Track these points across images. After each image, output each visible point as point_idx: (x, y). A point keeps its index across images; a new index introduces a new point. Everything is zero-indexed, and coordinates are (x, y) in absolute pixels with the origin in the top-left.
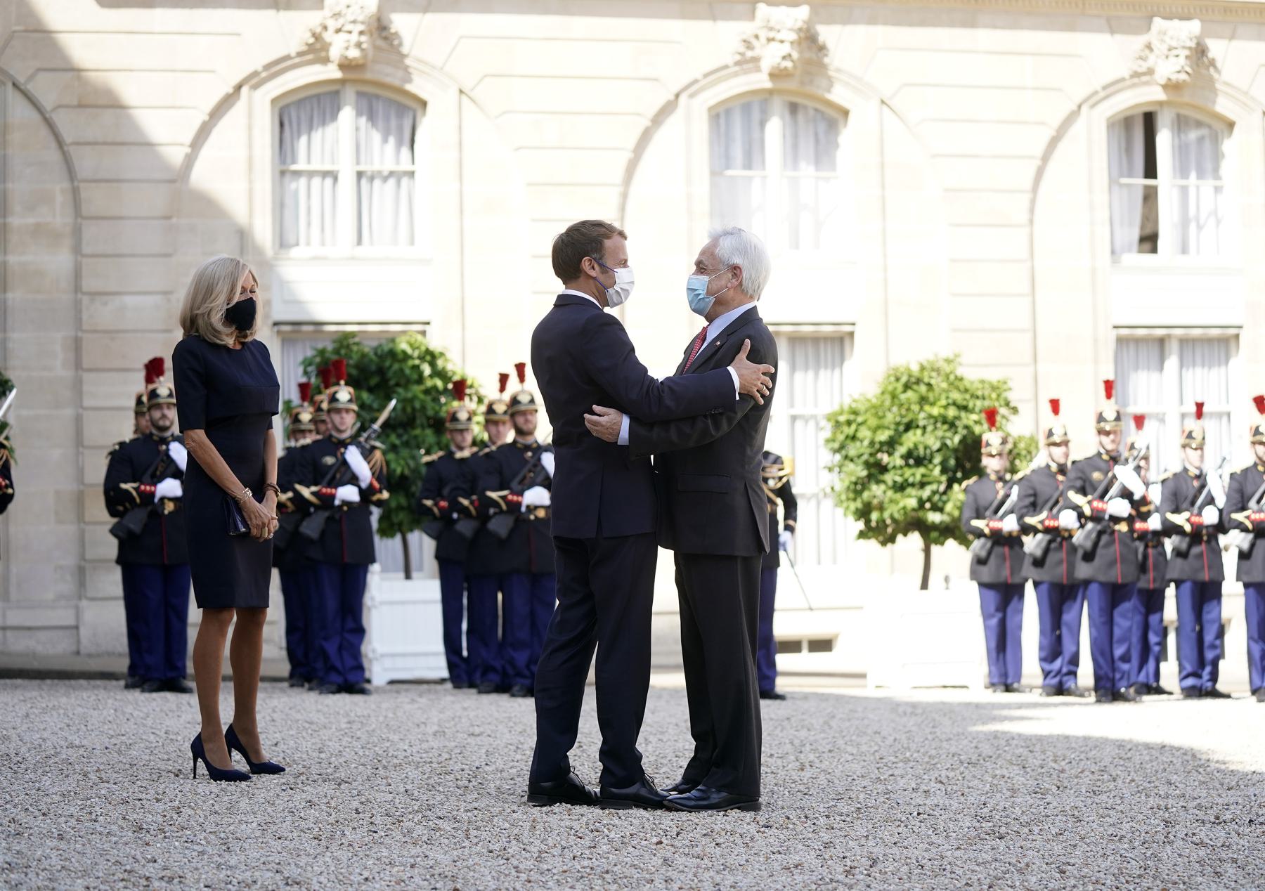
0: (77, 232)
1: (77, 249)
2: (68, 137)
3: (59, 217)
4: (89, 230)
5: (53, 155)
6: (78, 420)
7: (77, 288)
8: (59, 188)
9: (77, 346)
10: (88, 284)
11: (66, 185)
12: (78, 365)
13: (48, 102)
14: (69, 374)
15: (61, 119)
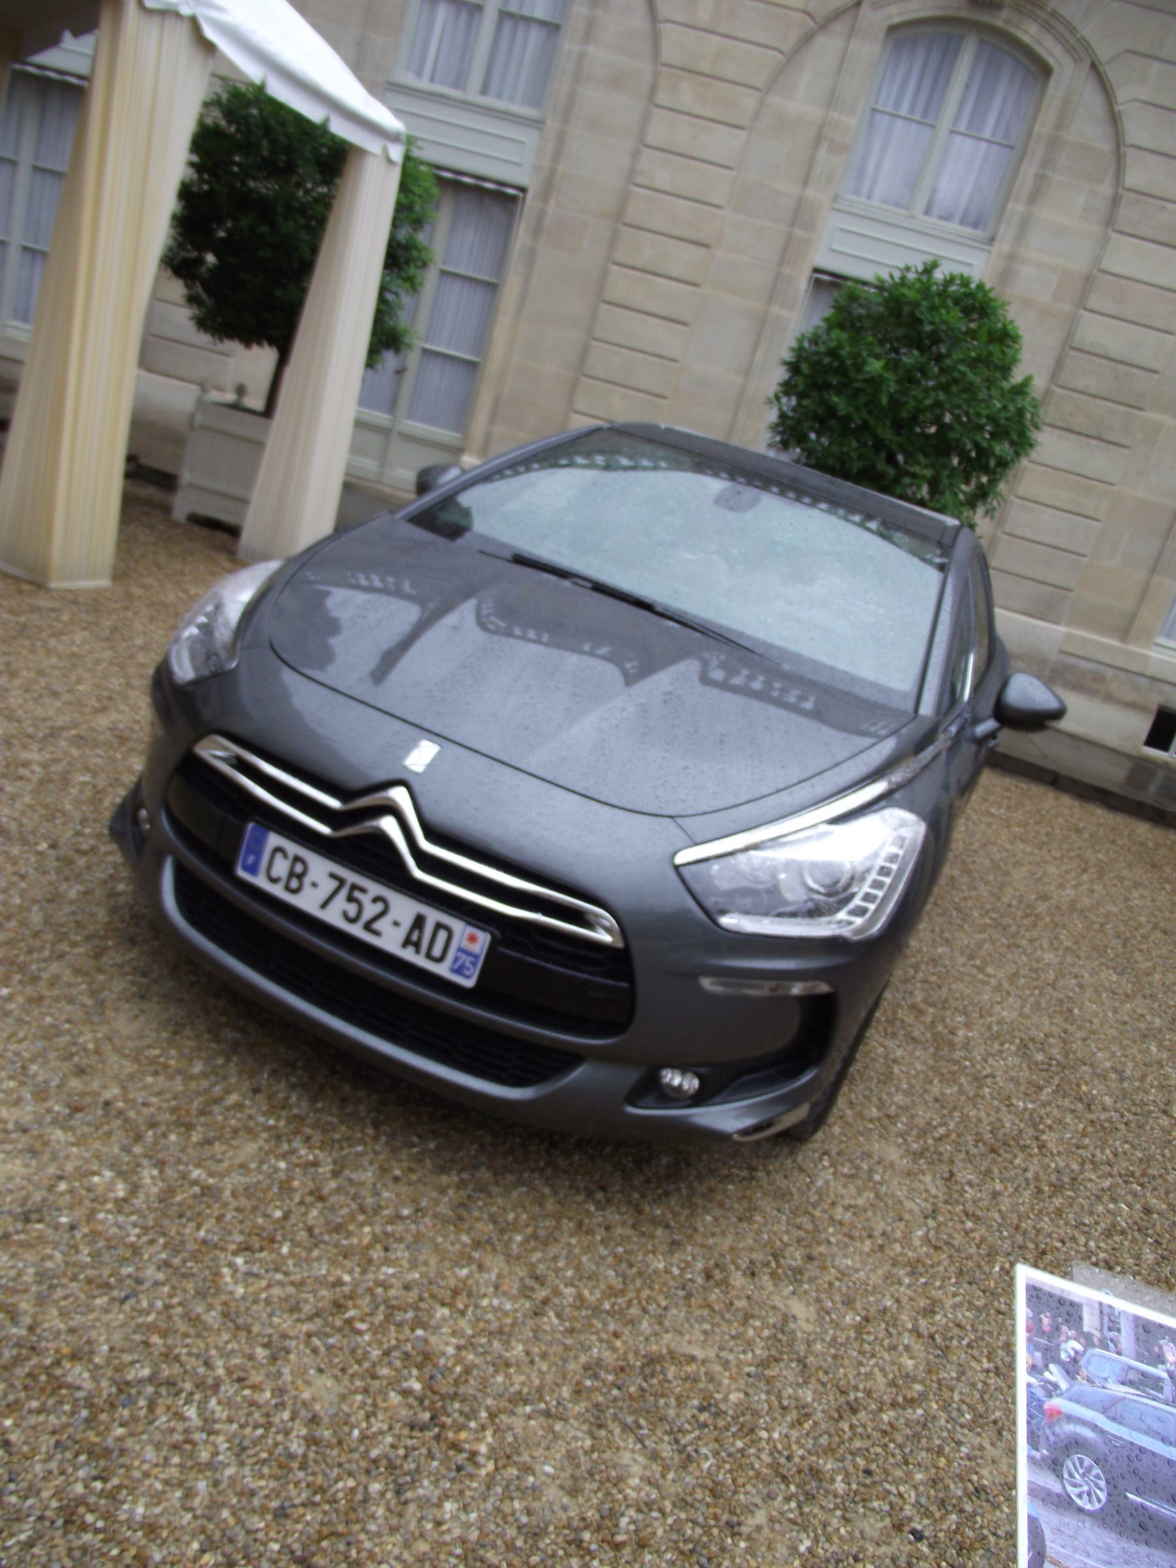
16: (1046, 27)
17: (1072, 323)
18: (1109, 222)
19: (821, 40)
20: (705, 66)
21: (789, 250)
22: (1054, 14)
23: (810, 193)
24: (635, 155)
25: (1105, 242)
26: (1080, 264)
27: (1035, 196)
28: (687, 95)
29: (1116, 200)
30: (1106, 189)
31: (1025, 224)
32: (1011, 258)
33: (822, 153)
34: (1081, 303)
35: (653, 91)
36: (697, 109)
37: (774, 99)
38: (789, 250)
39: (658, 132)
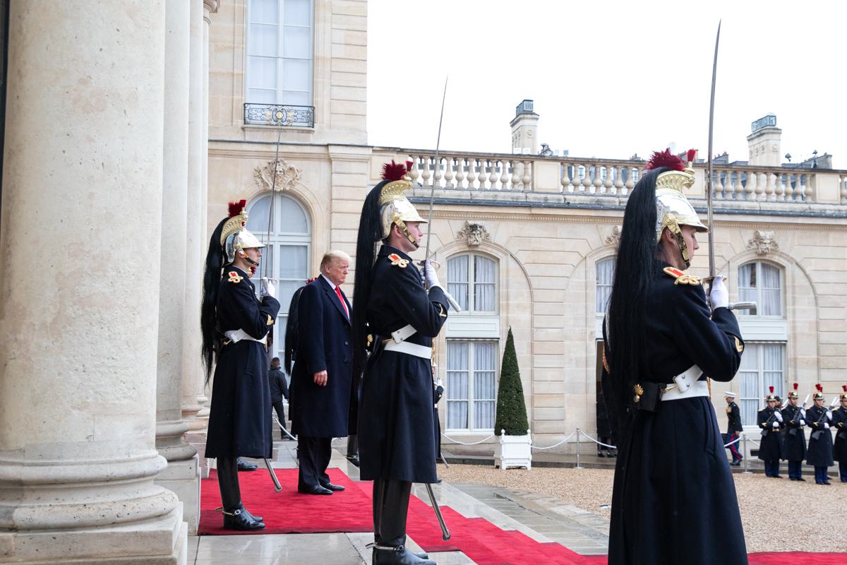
0: (532, 306)
1: (532, 312)
2: (529, 273)
3: (526, 301)
4: (537, 306)
5: (524, 280)
6: (532, 371)
7: (532, 326)
8: (526, 291)
9: (532, 346)
10: (536, 325)
11: (528, 290)
12: (532, 352)
13: (522, 262)
14: (529, 355)
15: (527, 268)
16: (780, 256)
18: (817, 304)
22: (781, 253)
26: (813, 318)
27: (794, 304)
29: (816, 298)
30: (812, 295)
31: (794, 311)
32: (794, 322)
34: (817, 330)
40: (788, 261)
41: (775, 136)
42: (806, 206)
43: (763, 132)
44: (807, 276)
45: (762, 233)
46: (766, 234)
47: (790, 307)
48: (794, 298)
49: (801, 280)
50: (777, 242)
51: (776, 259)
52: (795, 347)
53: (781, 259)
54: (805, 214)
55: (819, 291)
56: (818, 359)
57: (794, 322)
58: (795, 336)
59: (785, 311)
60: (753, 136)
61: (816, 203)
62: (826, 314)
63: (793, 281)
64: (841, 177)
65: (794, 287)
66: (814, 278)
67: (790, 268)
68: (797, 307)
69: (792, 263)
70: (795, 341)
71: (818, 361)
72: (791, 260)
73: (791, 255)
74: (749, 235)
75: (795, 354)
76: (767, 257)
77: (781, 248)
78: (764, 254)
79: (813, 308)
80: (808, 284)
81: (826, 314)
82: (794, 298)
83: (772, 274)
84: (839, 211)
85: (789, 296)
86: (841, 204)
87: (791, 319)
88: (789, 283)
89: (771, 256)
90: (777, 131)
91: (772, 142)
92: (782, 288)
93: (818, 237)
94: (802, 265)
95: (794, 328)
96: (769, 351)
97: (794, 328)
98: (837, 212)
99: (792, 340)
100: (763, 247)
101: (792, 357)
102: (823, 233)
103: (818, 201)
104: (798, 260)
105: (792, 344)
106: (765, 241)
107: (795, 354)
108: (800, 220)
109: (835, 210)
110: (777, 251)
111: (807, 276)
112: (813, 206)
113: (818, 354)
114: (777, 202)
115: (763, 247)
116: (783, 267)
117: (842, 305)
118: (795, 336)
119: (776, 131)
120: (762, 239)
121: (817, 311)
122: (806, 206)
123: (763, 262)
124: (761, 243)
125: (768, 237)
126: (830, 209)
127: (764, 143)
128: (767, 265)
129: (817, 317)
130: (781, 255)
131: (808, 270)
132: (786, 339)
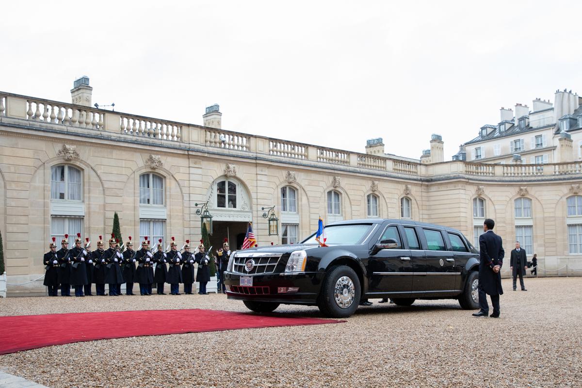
16: (80, 162)
17: (104, 214)
18: (104, 194)
19: (38, 171)
20: (16, 180)
21: (45, 213)
23: (46, 200)
24: (5, 200)
25: (105, 198)
26: (102, 203)
27: (89, 193)
28: (13, 186)
29: (104, 190)
30: (101, 188)
31: (89, 198)
32: (89, 204)
33: (46, 192)
34: (105, 210)
35: (5, 187)
36: (17, 189)
37: (32, 184)
38: (45, 213)
39: (9, 194)
40: (86, 166)
41: (88, 91)
42: (99, 132)
43: (80, 88)
44: (98, 176)
45: (68, 146)
46: (71, 147)
47: (86, 195)
48: (89, 189)
49: (94, 178)
50: (78, 153)
51: (78, 164)
52: (89, 220)
53: (82, 164)
54: (98, 137)
55: (106, 186)
56: (104, 228)
57: (89, 204)
58: (89, 213)
59: (84, 196)
60: (74, 90)
61: (105, 131)
62: (109, 200)
63: (89, 179)
64: (121, 117)
65: (89, 182)
66: (103, 178)
67: (87, 170)
68: (91, 195)
69: (88, 167)
70: (89, 217)
71: (104, 229)
72: (88, 165)
73: (88, 162)
74: (59, 147)
75: (89, 225)
76: (72, 162)
77: (81, 157)
78: (69, 160)
79: (102, 196)
80: (99, 181)
81: (109, 200)
82: (89, 189)
83: (75, 174)
84: (120, 137)
85: (86, 188)
86: (121, 134)
87: (87, 203)
88: (86, 180)
89: (74, 161)
90: (90, 89)
91: (85, 95)
92: (82, 183)
93: (105, 152)
94: (95, 169)
95: (89, 208)
96: (72, 223)
97: (89, 208)
98: (118, 138)
99: (87, 216)
100: (68, 155)
101: (88, 226)
102: (109, 150)
103: (106, 130)
104: (93, 165)
105: (87, 218)
106: (70, 152)
107: (89, 225)
108: (94, 141)
109: (117, 137)
110: (79, 159)
111: (98, 176)
112: (102, 133)
113: (104, 224)
114: (79, 128)
115: (68, 155)
116: (83, 170)
117: (121, 195)
118: (89, 213)
119: (89, 88)
120: (68, 150)
121: (105, 198)
122: (99, 132)
123: (69, 165)
124: (67, 152)
125: (72, 149)
126: (114, 136)
127: (80, 95)
128: (72, 167)
129: (105, 201)
130: (81, 161)
131: (99, 172)
132: (84, 215)
